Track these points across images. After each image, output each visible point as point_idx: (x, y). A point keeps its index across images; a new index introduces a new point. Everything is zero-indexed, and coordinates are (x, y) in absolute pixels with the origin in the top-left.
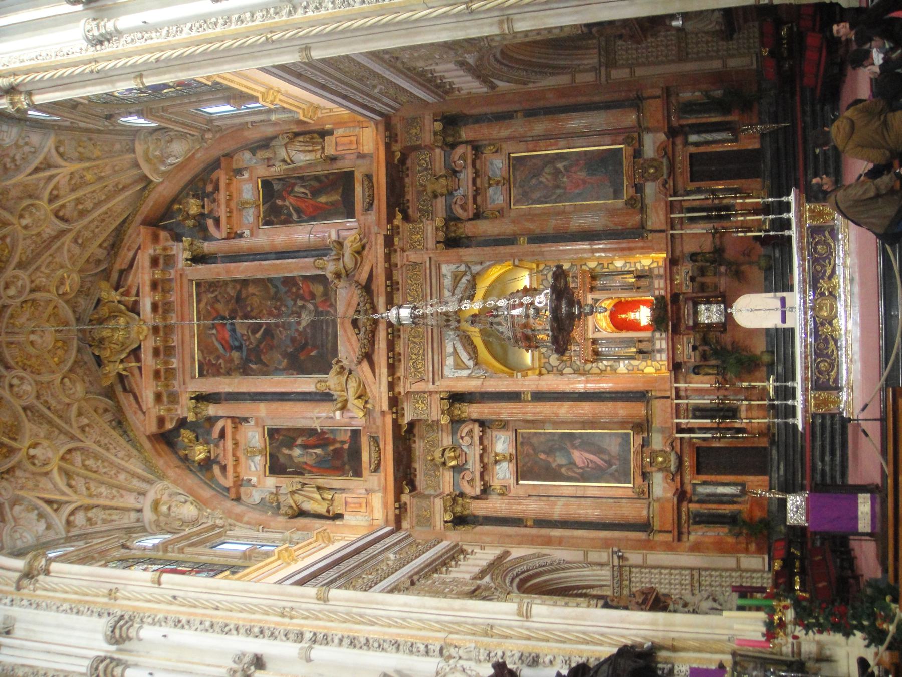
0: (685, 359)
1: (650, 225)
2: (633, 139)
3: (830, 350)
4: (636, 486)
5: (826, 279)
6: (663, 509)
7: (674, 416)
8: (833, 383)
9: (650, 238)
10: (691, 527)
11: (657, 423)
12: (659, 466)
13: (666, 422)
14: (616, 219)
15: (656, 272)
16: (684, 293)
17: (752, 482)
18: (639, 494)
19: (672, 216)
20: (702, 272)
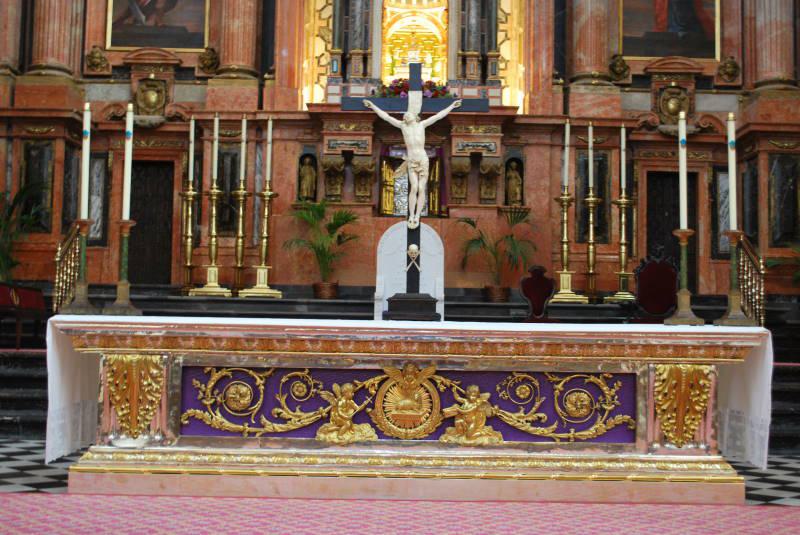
0: (326, 139)
1: (577, 89)
2: (733, 76)
3: (286, 413)
4: (104, 55)
5: (495, 410)
6: (55, 92)
7: (223, 117)
8: (191, 418)
9: (555, 88)
10: (20, 146)
11: (216, 85)
12: (140, 95)
13: (214, 103)
14: (591, 34)
15: (492, 92)
16: (450, 143)
17: (108, 257)
18: (91, 56)
19: (591, 129)
20: (490, 177)
